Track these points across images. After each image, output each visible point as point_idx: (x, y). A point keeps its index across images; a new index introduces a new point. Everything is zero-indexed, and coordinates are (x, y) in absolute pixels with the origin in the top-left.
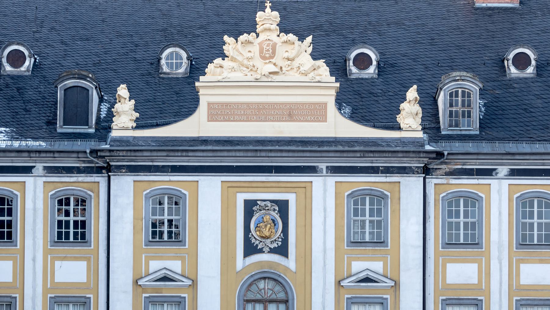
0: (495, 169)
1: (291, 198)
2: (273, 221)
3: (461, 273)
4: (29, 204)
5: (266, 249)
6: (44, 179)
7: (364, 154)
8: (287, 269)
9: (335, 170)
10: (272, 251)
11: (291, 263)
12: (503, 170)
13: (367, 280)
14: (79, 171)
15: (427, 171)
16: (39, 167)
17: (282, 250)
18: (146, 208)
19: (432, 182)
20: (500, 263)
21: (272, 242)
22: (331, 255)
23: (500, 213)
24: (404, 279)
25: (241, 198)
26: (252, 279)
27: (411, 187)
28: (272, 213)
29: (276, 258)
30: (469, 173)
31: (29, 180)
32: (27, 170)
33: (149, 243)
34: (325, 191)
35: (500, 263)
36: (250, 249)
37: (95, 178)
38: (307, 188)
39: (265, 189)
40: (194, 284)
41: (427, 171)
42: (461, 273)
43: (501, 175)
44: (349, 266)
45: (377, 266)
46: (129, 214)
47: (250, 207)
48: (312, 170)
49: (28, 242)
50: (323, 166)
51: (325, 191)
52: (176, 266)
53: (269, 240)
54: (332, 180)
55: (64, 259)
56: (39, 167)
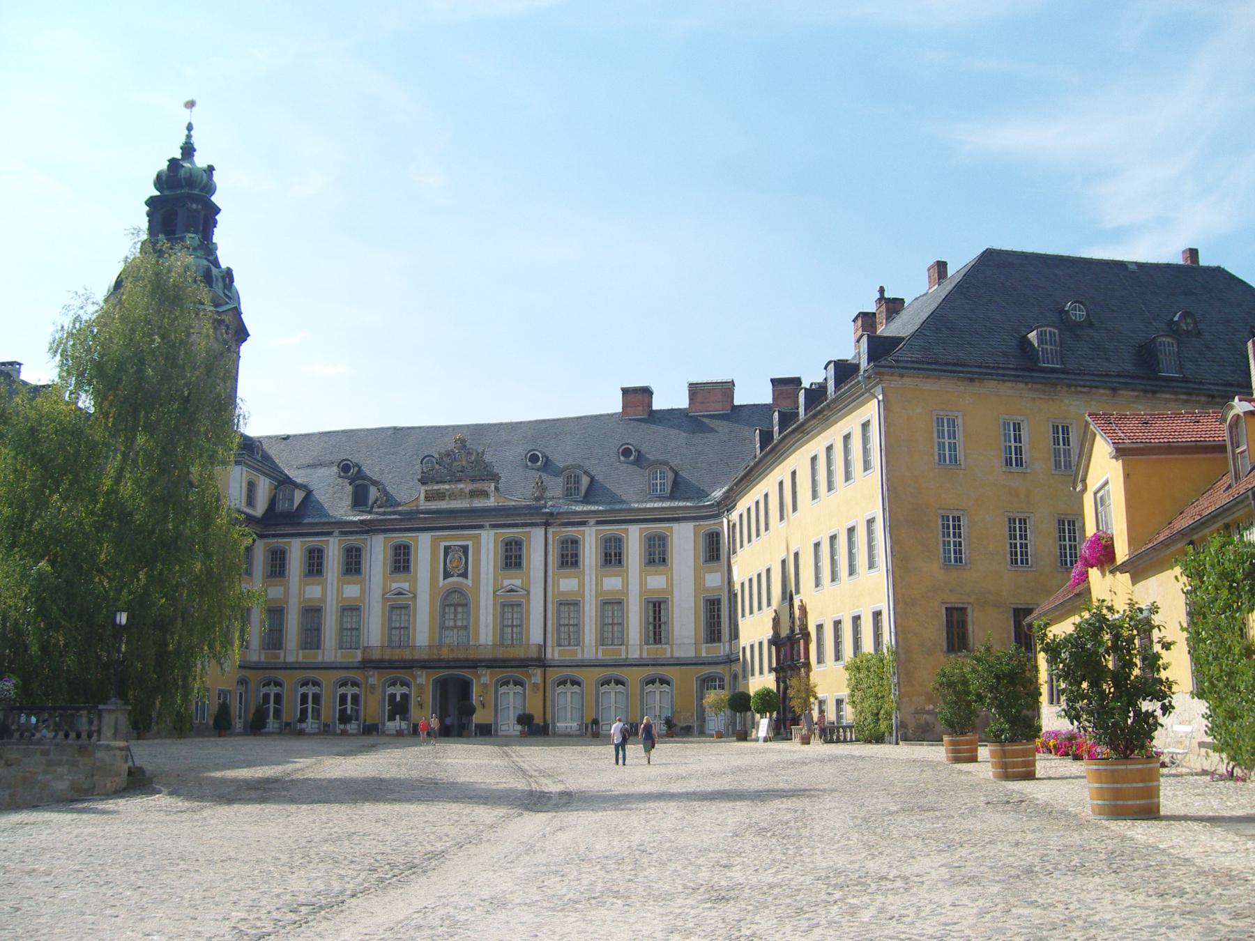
1: (470, 543)
4: (331, 554)
7: (508, 516)
9: (494, 526)
10: (459, 575)
11: (469, 582)
12: (592, 521)
14: (357, 533)
15: (547, 524)
16: (336, 532)
17: (465, 575)
18: (390, 553)
19: (551, 530)
24: (532, 590)
25: (443, 544)
27: (537, 535)
29: (461, 579)
31: (331, 539)
32: (329, 534)
33: (392, 572)
36: (447, 575)
37: (365, 536)
39: (455, 539)
40: (415, 597)
41: (547, 524)
42: (568, 584)
45: (518, 582)
46: (381, 557)
47: (447, 549)
48: (481, 527)
49: (330, 575)
52: (406, 586)
54: (492, 532)
55: (348, 583)
56: (336, 532)
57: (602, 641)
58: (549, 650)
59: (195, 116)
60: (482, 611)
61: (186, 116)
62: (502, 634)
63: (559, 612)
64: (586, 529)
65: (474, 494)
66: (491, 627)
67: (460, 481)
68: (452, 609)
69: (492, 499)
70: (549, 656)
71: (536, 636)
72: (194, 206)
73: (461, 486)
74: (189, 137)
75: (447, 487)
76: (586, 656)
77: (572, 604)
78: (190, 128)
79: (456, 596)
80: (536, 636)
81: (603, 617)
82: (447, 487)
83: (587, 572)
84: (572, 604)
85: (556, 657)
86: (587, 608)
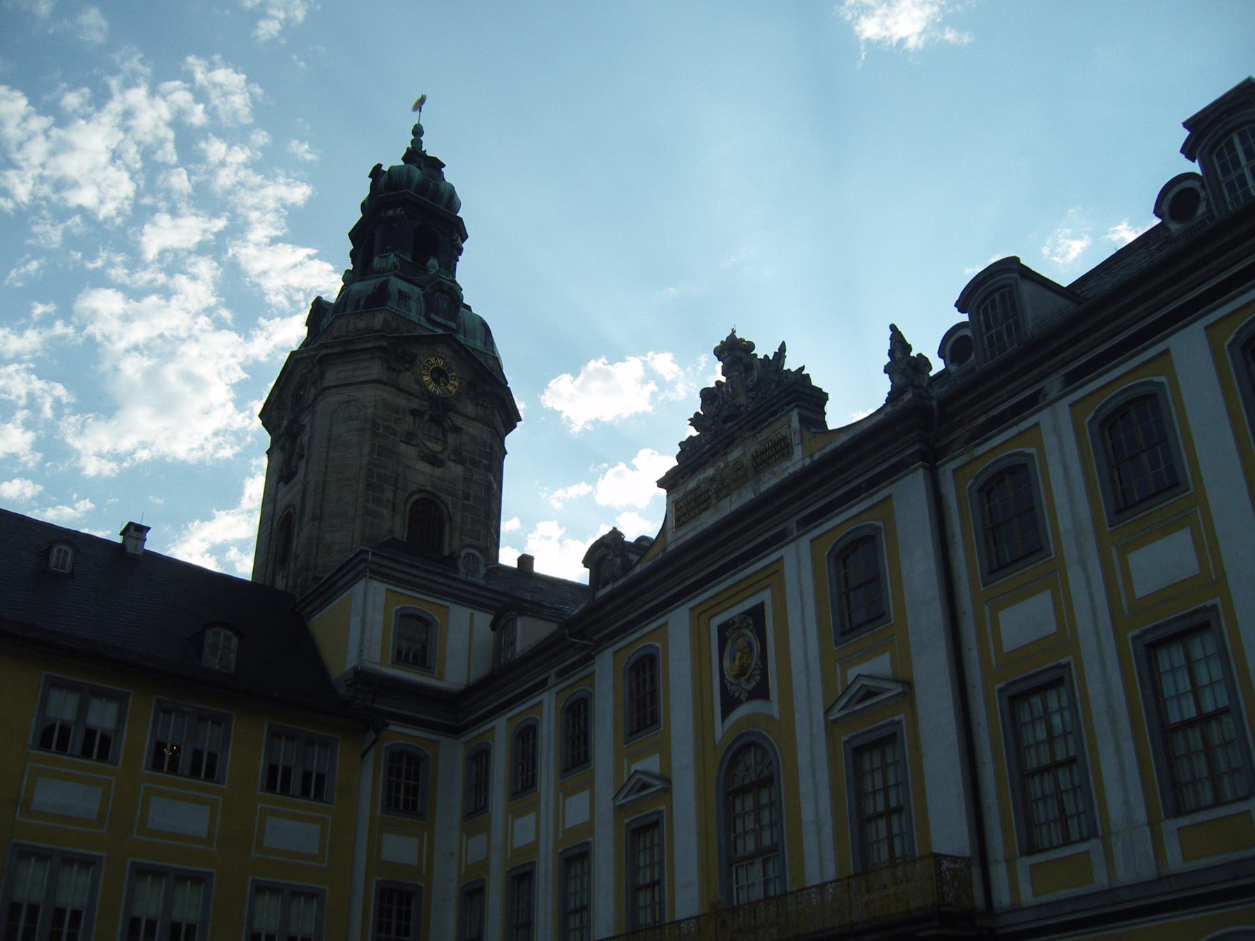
0: (1039, 392)
2: (750, 644)
3: (1024, 621)
5: (744, 696)
6: (556, 689)
8: (771, 717)
11: (774, 708)
13: (870, 694)
15: (931, 458)
20: (1085, 570)
21: (748, 680)
22: (816, 667)
23: (1066, 470)
26: (730, 753)
28: (747, 632)
30: (999, 422)
34: (799, 562)
35: (1085, 570)
38: (776, 569)
41: (931, 458)
42: (1024, 621)
43: (1053, 394)
44: (844, 676)
45: (881, 664)
50: (792, 524)
51: (799, 562)
53: (743, 679)
57: (1172, 793)
58: (999, 874)
59: (426, 119)
60: (805, 786)
61: (413, 119)
62: (863, 846)
63: (1014, 728)
64: (1043, 418)
65: (762, 461)
66: (828, 831)
67: (731, 443)
68: (749, 802)
69: (798, 452)
70: (1002, 897)
71: (948, 831)
72: (390, 213)
73: (736, 453)
74: (417, 142)
75: (710, 472)
76: (1125, 874)
77: (1042, 683)
78: (418, 131)
79: (751, 758)
80: (948, 831)
81: (1157, 702)
82: (710, 472)
83: (1070, 553)
84: (1042, 683)
85: (1027, 896)
86: (1094, 688)
